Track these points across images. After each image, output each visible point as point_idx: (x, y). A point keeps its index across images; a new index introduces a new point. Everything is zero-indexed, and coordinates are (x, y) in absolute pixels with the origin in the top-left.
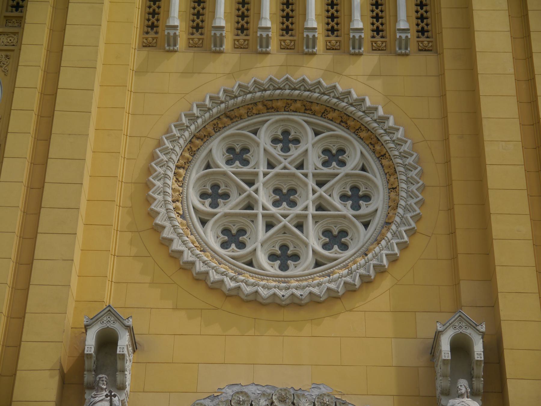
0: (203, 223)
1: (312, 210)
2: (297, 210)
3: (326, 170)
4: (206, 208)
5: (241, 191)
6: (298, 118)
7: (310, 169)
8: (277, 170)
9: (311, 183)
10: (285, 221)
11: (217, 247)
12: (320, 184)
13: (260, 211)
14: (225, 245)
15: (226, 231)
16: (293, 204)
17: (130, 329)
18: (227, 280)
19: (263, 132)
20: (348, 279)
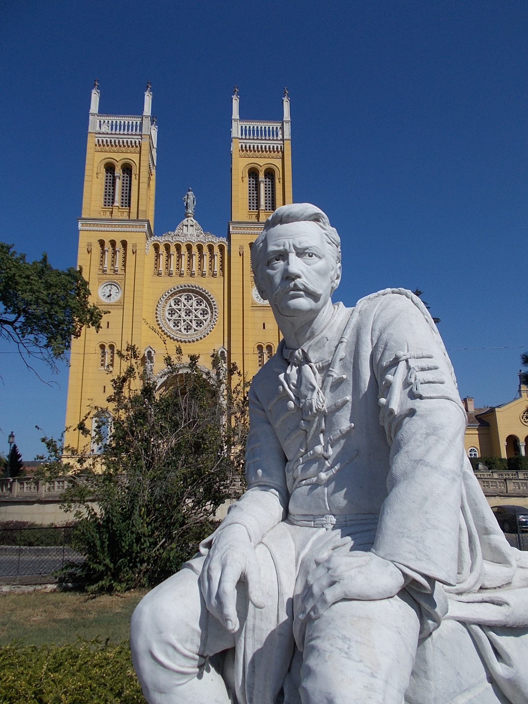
0: (169, 321)
1: (194, 318)
2: (190, 318)
3: (197, 307)
4: (170, 318)
5: (178, 313)
6: (191, 294)
7: (194, 307)
8: (186, 308)
9: (194, 311)
10: (187, 321)
11: (172, 327)
12: (196, 311)
13: (182, 318)
14: (174, 326)
15: (174, 323)
16: (189, 316)
17: (154, 351)
18: (174, 337)
19: (182, 297)
20: (201, 336)
